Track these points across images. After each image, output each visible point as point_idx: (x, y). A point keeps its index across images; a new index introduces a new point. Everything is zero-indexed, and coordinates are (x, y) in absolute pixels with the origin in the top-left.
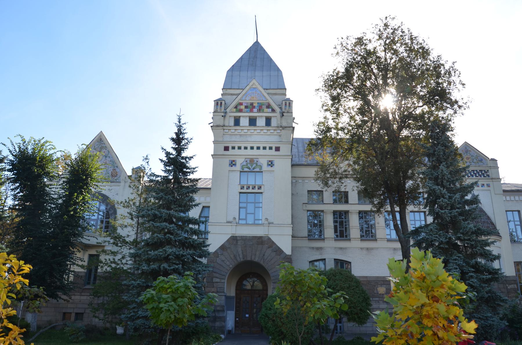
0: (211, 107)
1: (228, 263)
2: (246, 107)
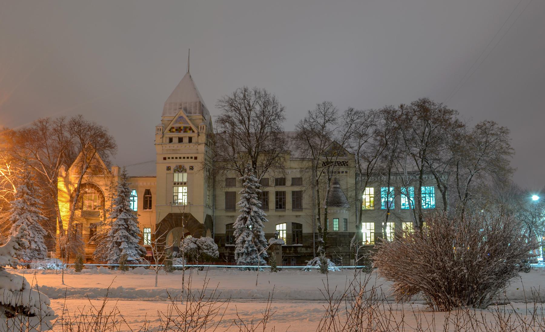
2: (176, 130)
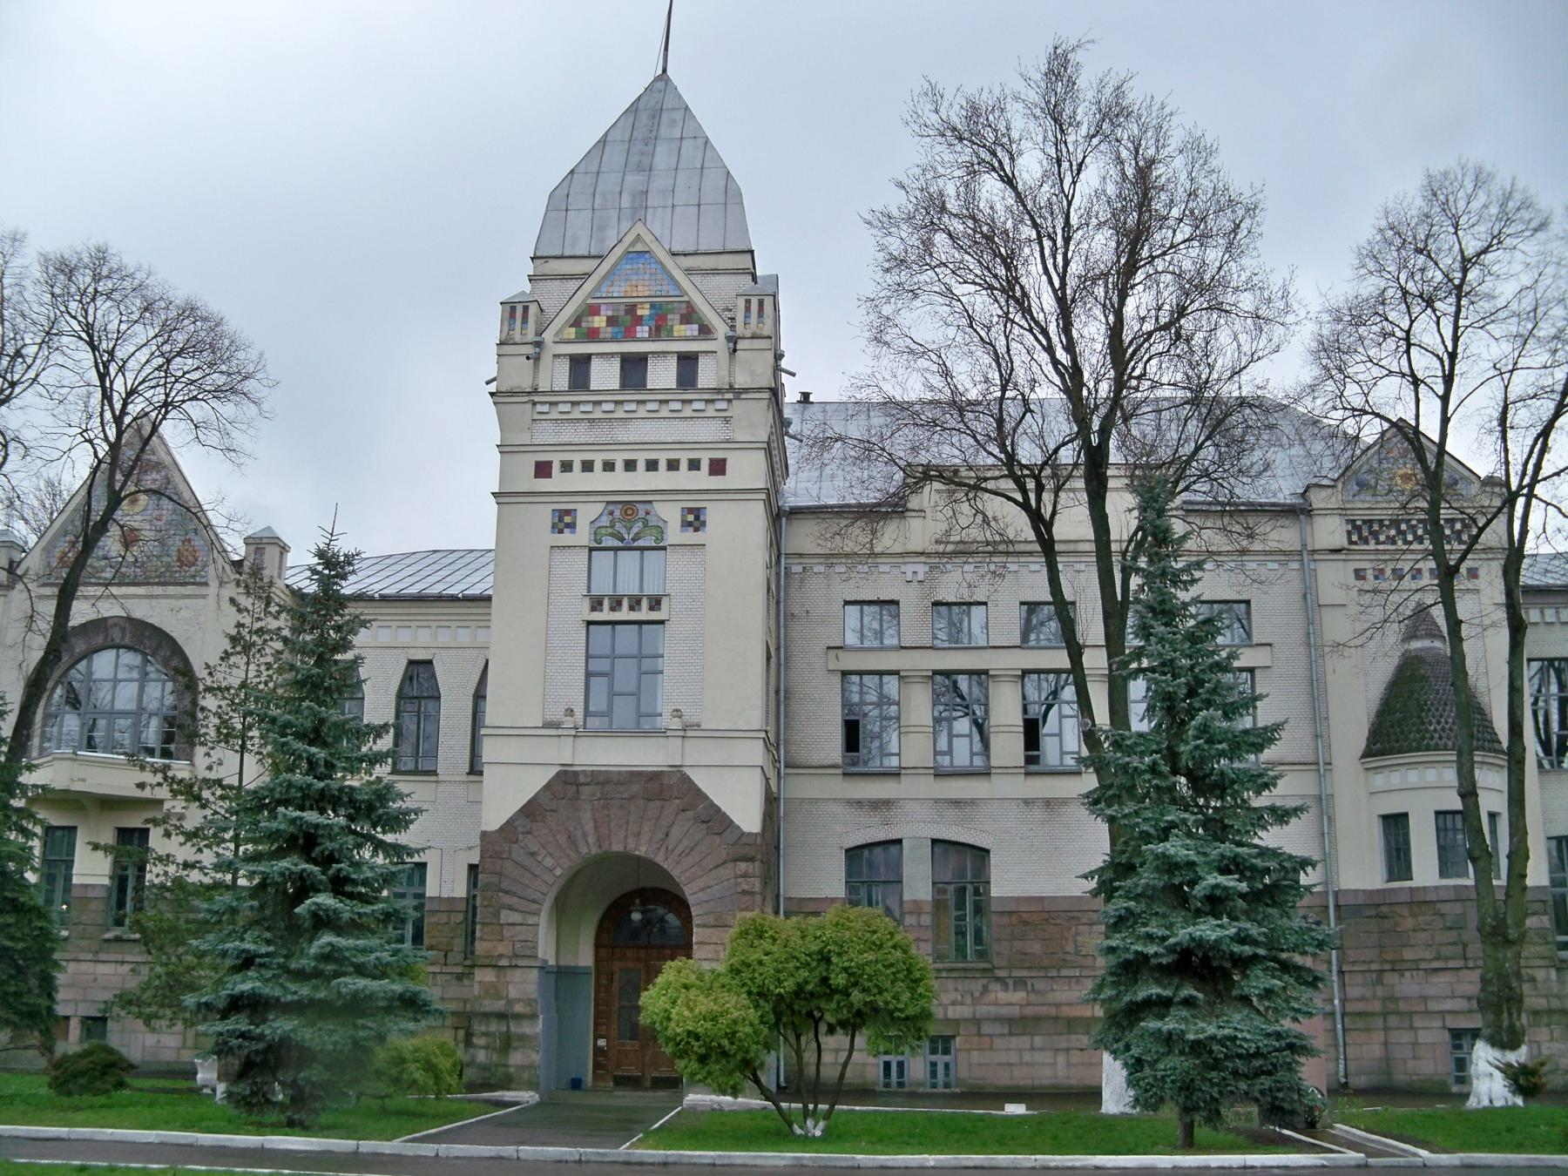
0: (492, 326)
1: (549, 862)
2: (611, 321)
